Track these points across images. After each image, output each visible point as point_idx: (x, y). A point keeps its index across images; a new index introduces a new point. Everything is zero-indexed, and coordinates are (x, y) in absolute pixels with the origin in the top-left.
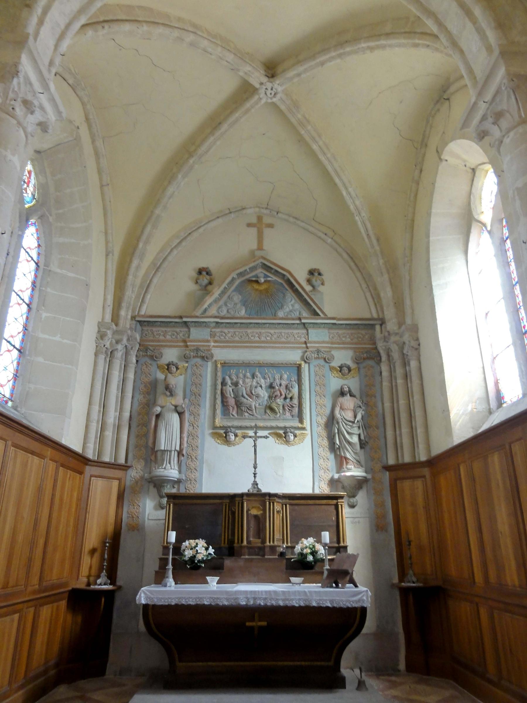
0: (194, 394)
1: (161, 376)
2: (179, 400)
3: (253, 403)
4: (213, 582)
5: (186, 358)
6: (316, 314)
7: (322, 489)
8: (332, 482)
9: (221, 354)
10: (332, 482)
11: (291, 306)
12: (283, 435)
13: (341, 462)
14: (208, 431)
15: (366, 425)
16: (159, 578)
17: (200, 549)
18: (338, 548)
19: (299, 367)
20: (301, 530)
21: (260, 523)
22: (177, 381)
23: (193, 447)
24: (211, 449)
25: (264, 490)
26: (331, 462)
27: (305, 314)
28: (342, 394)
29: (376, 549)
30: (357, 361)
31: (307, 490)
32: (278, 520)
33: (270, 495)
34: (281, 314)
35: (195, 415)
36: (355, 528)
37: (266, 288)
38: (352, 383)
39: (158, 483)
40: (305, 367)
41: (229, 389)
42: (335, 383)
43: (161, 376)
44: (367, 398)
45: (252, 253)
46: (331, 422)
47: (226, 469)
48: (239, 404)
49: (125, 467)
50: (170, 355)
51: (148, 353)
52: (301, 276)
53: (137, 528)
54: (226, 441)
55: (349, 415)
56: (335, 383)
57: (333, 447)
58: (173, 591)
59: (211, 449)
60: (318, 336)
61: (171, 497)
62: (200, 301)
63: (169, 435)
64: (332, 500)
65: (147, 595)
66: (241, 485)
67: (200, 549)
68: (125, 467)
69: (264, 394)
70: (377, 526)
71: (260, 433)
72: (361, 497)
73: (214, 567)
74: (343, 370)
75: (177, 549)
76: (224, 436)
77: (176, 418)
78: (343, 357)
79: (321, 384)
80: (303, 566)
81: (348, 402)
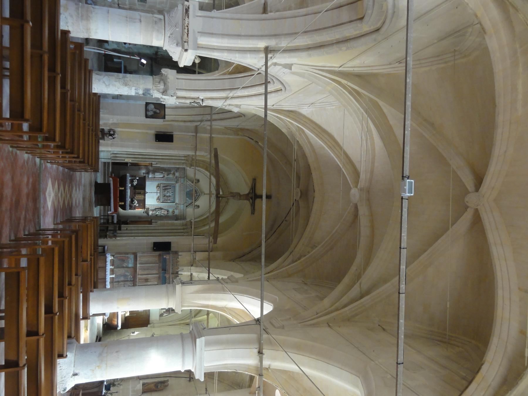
0: (167, 179)
1: (172, 173)
2: (166, 176)
3: (166, 192)
4: (130, 185)
5: (176, 177)
6: (186, 207)
7: (147, 206)
8: (148, 208)
9: (177, 186)
10: (148, 208)
11: (190, 201)
12: (158, 199)
13: (153, 210)
14: (159, 183)
15: (161, 216)
16: (131, 176)
17: (135, 183)
18: (135, 208)
19: (174, 202)
20: (139, 202)
21: (140, 193)
22: (171, 176)
23: (156, 180)
24: (156, 183)
25: (146, 195)
26: (153, 208)
27: (187, 204)
28: (168, 211)
29: (134, 217)
30: (176, 215)
31: (146, 203)
32: (140, 197)
33: (145, 196)
34: (187, 199)
35: (163, 180)
36: (139, 211)
37: (193, 195)
38: (170, 214)
39: (148, 173)
40: (174, 204)
41: (169, 187)
42: (171, 210)
43: (172, 173)
44: (166, 217)
45: (204, 192)
46: (161, 209)
47: (151, 187)
48: (166, 189)
49: (152, 166)
50: (177, 174)
51: (177, 169)
52: (197, 203)
53: (140, 169)
54: (157, 186)
55: (163, 212)
56: (171, 210)
57: (156, 209)
58: (129, 178)
59: (156, 183)
60: (182, 206)
61: (145, 177)
62: (190, 180)
63: (158, 175)
64: (144, 206)
65: (128, 175)
66: (147, 189)
67: (135, 183)
68: (152, 166)
69: (168, 195)
70: (140, 217)
71: (159, 194)
72: (145, 214)
73: (132, 185)
74: (173, 212)
75: (134, 179)
76: (158, 186)
77: (162, 176)
78: (177, 212)
79: (170, 207)
80: (132, 201)
81: (166, 213)
